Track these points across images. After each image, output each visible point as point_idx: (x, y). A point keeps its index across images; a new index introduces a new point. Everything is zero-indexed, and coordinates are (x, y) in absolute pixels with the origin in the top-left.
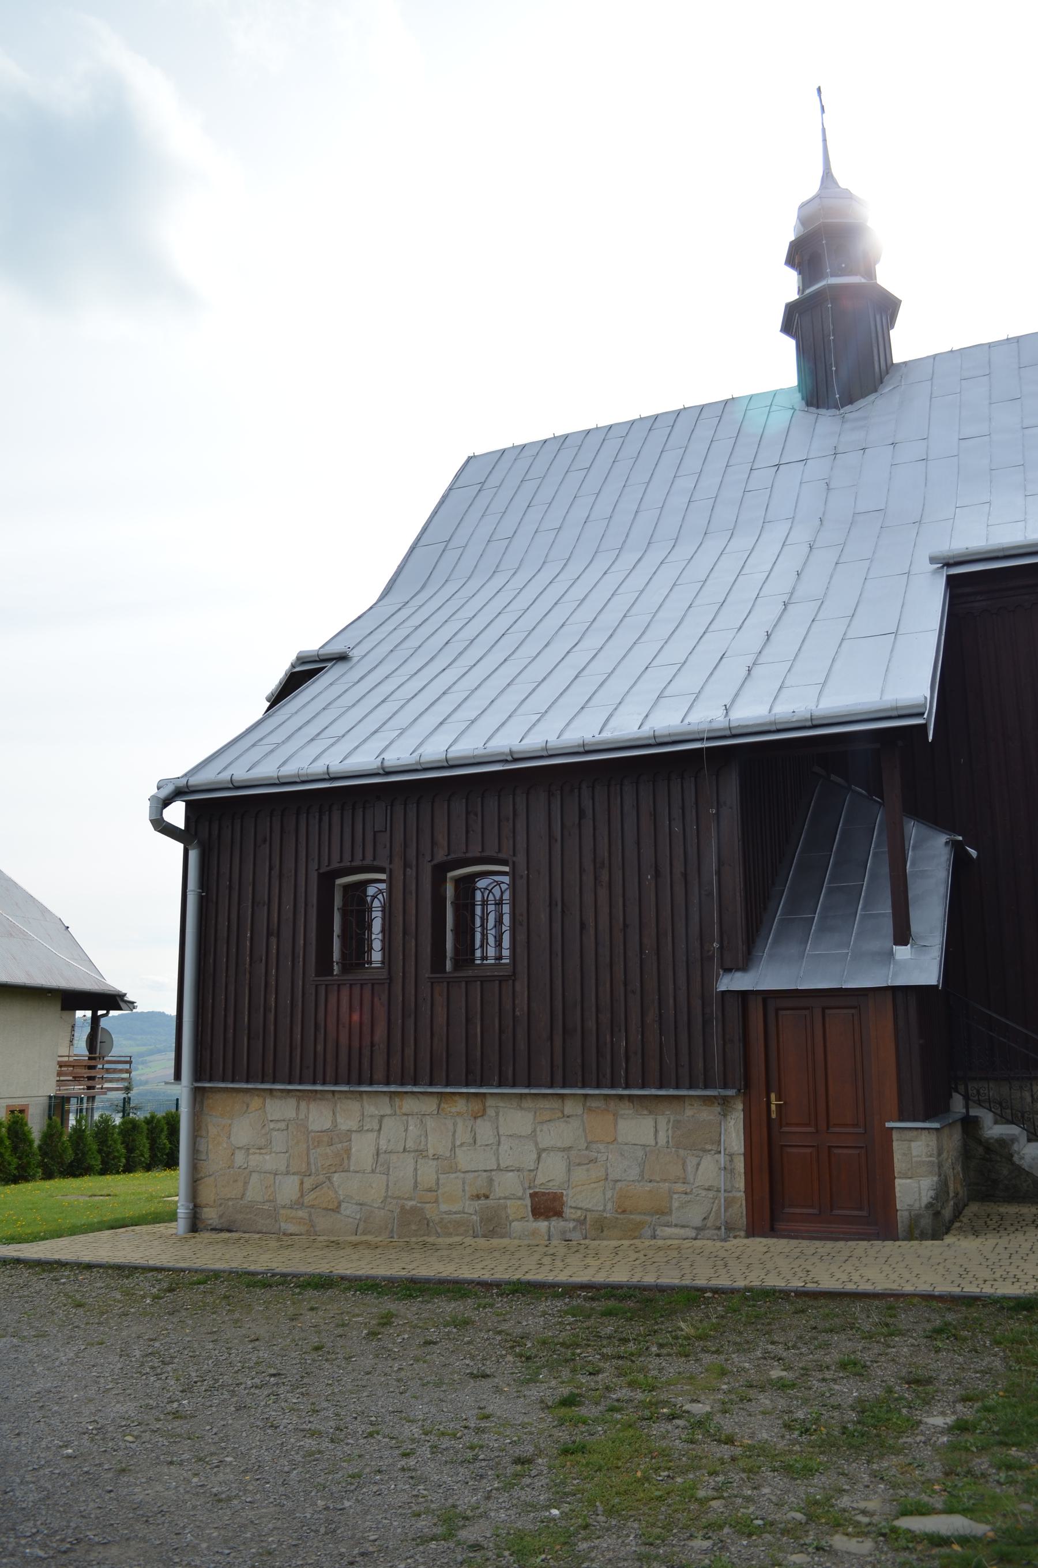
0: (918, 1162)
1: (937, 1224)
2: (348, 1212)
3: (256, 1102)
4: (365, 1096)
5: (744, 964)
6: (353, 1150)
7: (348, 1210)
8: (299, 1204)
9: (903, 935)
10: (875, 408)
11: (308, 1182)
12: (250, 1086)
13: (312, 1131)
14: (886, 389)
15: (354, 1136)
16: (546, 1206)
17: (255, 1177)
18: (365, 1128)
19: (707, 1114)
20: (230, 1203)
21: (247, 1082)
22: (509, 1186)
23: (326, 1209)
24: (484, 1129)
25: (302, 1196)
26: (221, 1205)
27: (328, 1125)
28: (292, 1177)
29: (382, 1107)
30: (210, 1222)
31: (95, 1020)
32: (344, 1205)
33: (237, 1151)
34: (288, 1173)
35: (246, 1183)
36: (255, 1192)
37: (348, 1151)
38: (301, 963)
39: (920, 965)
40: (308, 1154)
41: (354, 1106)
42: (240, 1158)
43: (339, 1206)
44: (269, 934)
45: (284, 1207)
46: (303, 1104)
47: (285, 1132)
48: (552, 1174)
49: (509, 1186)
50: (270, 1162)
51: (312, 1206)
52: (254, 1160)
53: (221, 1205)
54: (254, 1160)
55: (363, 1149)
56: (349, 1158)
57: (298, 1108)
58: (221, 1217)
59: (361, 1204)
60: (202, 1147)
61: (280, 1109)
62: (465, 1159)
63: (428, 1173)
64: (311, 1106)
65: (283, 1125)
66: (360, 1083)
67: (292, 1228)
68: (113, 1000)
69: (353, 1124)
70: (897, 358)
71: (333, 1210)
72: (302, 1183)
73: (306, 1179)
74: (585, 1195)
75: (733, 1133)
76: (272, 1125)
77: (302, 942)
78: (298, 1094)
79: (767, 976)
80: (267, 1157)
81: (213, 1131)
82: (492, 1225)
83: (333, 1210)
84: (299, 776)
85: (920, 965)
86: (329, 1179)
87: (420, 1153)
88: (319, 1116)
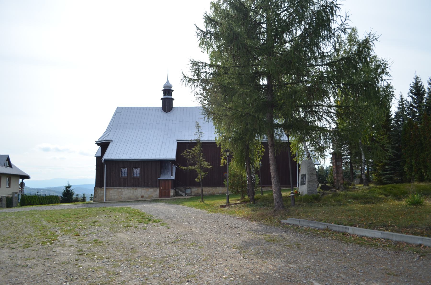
0: (172, 192)
1: (173, 196)
5: (160, 177)
9: (172, 175)
10: (171, 113)
14: (172, 111)
16: (142, 197)
19: (156, 189)
22: (139, 195)
24: (137, 191)
29: (127, 189)
31: (22, 180)
36: (113, 197)
39: (173, 178)
48: (143, 194)
49: (139, 195)
50: (114, 194)
55: (124, 193)
62: (135, 193)
63: (131, 194)
68: (28, 177)
70: (174, 106)
74: (146, 196)
75: (158, 190)
79: (162, 178)
82: (137, 198)
85: (173, 178)
87: (130, 193)
88: (120, 190)
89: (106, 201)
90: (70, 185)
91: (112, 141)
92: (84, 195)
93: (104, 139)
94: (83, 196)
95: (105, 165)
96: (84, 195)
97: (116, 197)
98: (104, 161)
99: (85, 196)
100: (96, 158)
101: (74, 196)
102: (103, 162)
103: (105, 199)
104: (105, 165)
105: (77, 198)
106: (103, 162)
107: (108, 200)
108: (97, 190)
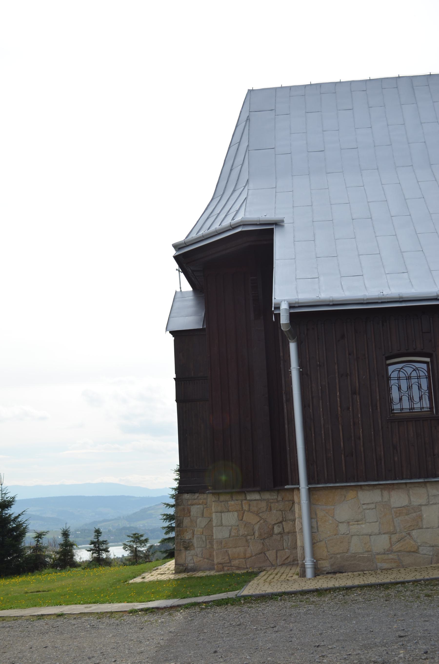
2: (425, 552)
3: (351, 494)
4: (428, 485)
6: (424, 516)
7: (424, 550)
8: (390, 551)
11: (394, 538)
12: (349, 484)
13: (394, 508)
15: (423, 508)
17: (355, 540)
18: (431, 503)
20: (339, 556)
21: (346, 482)
23: (410, 552)
25: (391, 546)
26: (331, 558)
27: (406, 503)
28: (384, 536)
30: (325, 569)
32: (421, 548)
33: (340, 525)
34: (380, 534)
35: (349, 543)
36: (356, 546)
37: (421, 517)
38: (379, 410)
40: (393, 521)
41: (422, 491)
42: (343, 528)
43: (418, 548)
44: (354, 393)
45: (378, 554)
46: (385, 493)
47: (374, 510)
50: (365, 528)
51: (399, 551)
52: (354, 528)
53: (331, 558)
54: (354, 528)
56: (422, 520)
57: (382, 496)
58: (332, 565)
59: (433, 546)
60: (314, 525)
61: (369, 497)
64: (411, 492)
65: (373, 506)
66: (428, 477)
67: (385, 566)
69: (423, 501)
71: (414, 552)
72: (390, 539)
73: (393, 536)
76: (365, 507)
77: (378, 397)
78: (381, 487)
80: (363, 526)
81: (320, 514)
83: (414, 552)
84: (381, 299)
86: (409, 534)
88: (398, 498)
89: (317, 572)
90: (10, 495)
91: (278, 223)
92: (66, 534)
93: (227, 222)
94: (60, 539)
95: (293, 347)
96: (66, 534)
97: (381, 543)
98: (292, 316)
99: (71, 539)
100: (171, 339)
101: (29, 540)
102: (284, 320)
103: (308, 563)
104: (293, 347)
105: (38, 548)
106: (284, 320)
107: (326, 565)
108: (195, 510)
